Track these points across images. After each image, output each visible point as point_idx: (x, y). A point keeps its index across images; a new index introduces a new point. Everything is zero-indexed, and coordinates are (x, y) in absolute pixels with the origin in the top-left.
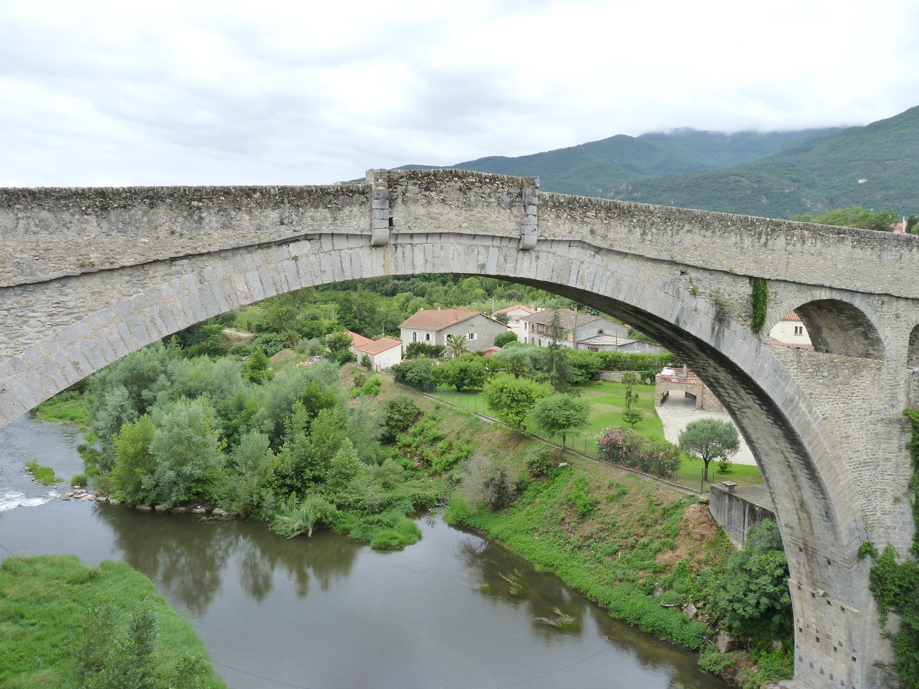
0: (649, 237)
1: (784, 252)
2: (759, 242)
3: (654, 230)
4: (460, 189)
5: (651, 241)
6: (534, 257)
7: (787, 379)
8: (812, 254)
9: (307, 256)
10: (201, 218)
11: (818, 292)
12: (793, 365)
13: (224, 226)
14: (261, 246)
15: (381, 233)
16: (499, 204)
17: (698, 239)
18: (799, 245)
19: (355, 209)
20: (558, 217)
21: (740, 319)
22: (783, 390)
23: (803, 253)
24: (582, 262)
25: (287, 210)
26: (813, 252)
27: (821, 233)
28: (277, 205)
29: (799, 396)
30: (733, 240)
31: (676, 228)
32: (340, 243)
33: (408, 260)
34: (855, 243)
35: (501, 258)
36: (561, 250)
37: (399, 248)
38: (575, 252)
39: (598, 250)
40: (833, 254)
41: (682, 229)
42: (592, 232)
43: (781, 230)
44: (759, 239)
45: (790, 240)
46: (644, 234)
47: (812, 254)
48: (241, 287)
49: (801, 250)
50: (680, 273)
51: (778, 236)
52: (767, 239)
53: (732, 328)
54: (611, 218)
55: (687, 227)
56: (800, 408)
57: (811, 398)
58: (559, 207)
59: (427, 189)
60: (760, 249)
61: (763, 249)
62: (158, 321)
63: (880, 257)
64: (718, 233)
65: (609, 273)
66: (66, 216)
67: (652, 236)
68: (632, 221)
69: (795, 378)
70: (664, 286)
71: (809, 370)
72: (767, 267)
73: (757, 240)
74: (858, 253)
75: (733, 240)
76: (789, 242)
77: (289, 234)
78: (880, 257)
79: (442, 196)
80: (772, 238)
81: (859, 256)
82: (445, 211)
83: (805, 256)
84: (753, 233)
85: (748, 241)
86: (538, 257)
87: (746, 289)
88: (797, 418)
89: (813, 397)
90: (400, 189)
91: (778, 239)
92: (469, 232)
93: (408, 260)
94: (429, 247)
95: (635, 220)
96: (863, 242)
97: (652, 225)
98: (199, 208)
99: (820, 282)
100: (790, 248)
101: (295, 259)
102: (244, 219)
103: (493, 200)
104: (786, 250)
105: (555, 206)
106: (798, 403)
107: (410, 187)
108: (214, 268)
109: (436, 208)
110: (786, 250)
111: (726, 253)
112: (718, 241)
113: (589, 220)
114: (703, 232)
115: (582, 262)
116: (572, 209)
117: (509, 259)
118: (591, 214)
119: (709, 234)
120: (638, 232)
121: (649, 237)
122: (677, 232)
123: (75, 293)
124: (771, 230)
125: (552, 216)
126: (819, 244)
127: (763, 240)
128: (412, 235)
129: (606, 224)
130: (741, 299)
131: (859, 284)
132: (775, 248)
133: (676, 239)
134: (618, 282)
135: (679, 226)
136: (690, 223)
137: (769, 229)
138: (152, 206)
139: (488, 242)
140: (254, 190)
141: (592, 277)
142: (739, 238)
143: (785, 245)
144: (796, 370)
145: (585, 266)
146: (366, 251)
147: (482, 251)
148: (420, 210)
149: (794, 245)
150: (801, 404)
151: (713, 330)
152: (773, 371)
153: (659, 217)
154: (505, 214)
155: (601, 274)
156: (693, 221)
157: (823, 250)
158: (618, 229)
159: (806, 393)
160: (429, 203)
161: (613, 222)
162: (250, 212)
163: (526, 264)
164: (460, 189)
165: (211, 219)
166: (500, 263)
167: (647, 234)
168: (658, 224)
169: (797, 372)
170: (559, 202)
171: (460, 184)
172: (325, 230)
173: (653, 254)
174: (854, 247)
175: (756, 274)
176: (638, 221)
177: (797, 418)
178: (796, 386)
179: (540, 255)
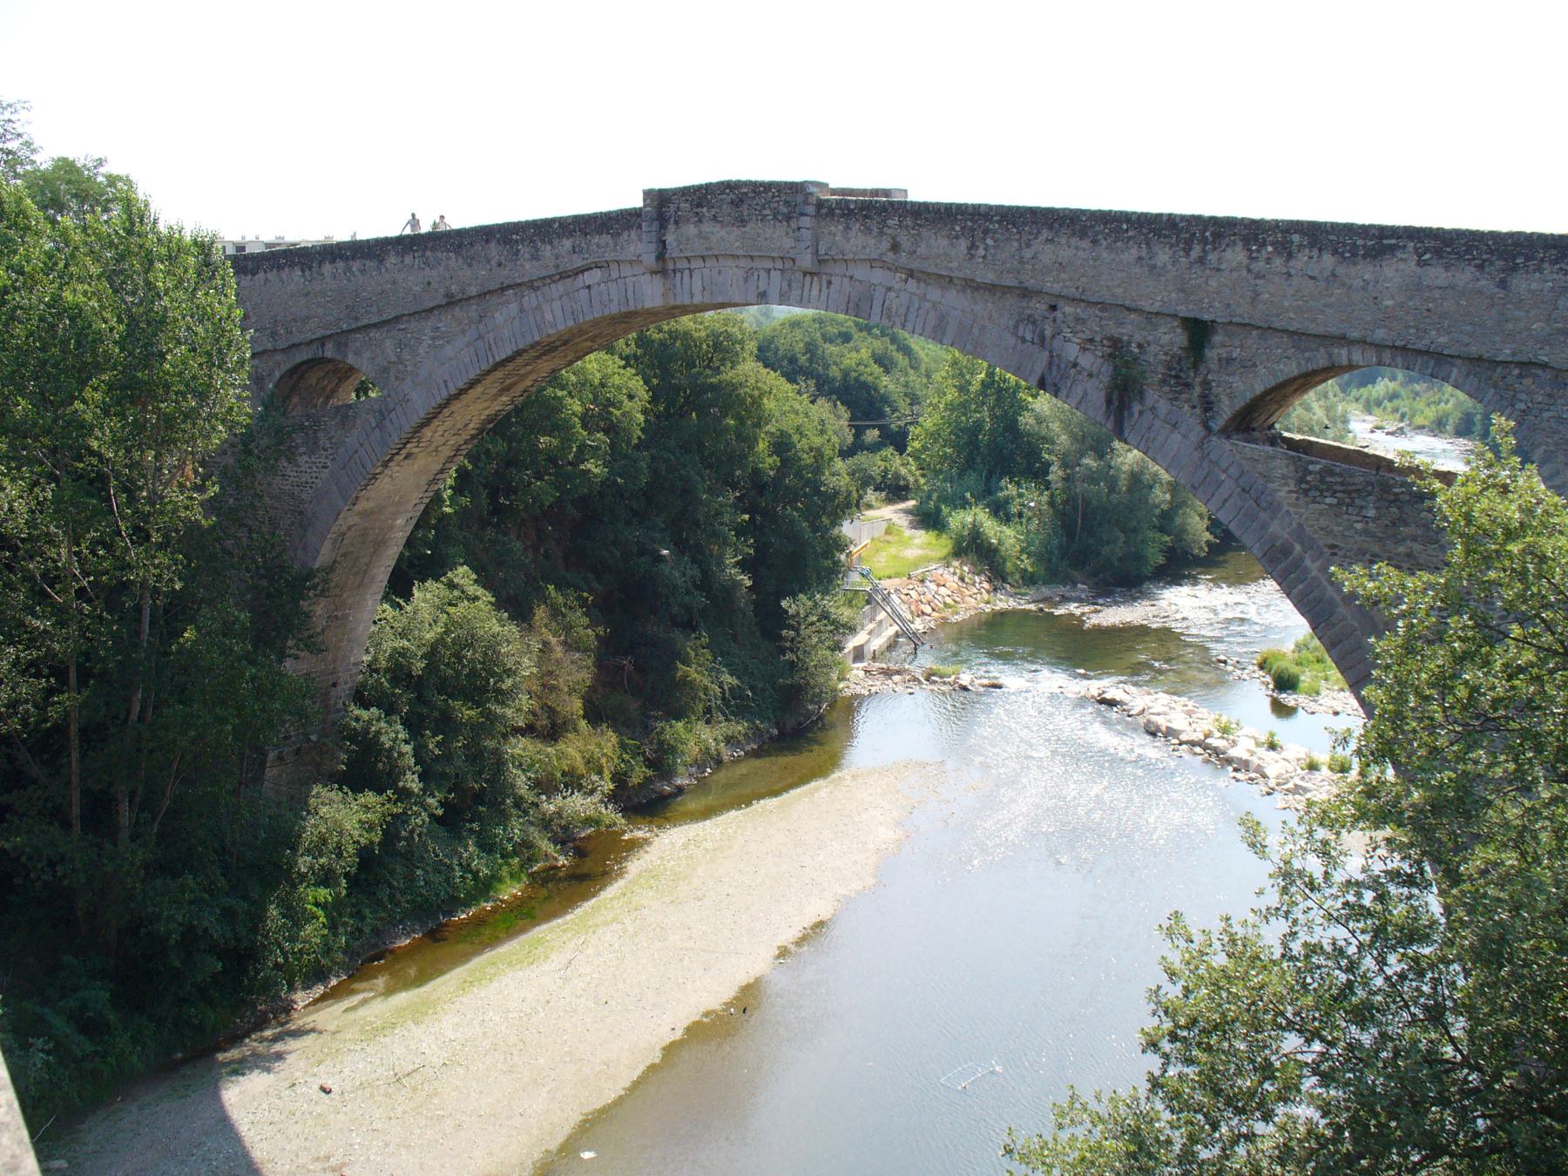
0: (981, 252)
1: (1245, 273)
2: (1188, 255)
3: (989, 242)
4: (732, 203)
5: (984, 257)
6: (824, 283)
7: (1274, 508)
8: (1311, 278)
9: (599, 284)
10: (518, 251)
11: (1344, 352)
12: (1286, 484)
13: (535, 257)
14: (564, 276)
15: (650, 259)
16: (775, 218)
17: (1065, 254)
18: (1278, 262)
19: (633, 233)
20: (847, 228)
21: (1166, 389)
22: (1264, 526)
23: (1289, 275)
24: (889, 289)
25: (578, 239)
26: (1315, 273)
27: (1331, 237)
28: (571, 235)
29: (1302, 544)
30: (1134, 252)
31: (1025, 238)
32: (626, 270)
33: (687, 287)
34: (1427, 256)
35: (785, 284)
36: (860, 272)
37: (678, 275)
38: (878, 276)
39: (911, 274)
40: (1367, 277)
41: (1036, 238)
42: (895, 247)
43: (1235, 234)
44: (1187, 252)
45: (1258, 251)
46: (973, 246)
47: (1311, 278)
48: (548, 317)
49: (1285, 270)
50: (1044, 307)
51: (1228, 245)
52: (1204, 250)
53: (1149, 402)
54: (920, 226)
55: (1046, 234)
56: (1306, 571)
57: (1335, 554)
58: (848, 215)
59: (699, 205)
60: (1190, 268)
61: (1197, 269)
62: (493, 347)
63: (1503, 284)
64: (1104, 243)
65: (928, 305)
66: (439, 254)
67: (986, 249)
68: (953, 229)
69: (1292, 510)
70: (1016, 327)
71: (1328, 500)
72: (1206, 301)
73: (1182, 253)
74: (1437, 275)
75: (1134, 252)
76: (1254, 255)
77: (578, 262)
78: (1503, 284)
79: (713, 211)
80: (1215, 249)
81: (1439, 282)
82: (717, 229)
83: (1295, 281)
84: (1174, 241)
85: (1163, 256)
86: (829, 283)
87: (1172, 338)
88: (1301, 587)
89: (1340, 553)
90: (672, 207)
91: (1229, 250)
92: (741, 252)
93: (687, 287)
94: (706, 271)
95: (957, 228)
96: (1450, 253)
97: (986, 232)
98: (516, 241)
99: (1333, 330)
100: (1260, 266)
101: (589, 287)
102: (546, 251)
103: (767, 212)
104: (1249, 271)
105: (843, 215)
106: (1302, 559)
107: (682, 205)
108: (530, 299)
109: (707, 227)
110: (1249, 271)
111: (1119, 275)
112: (1105, 254)
113: (890, 231)
114: (1074, 241)
115: (889, 289)
116: (866, 217)
117: (793, 284)
118: (890, 222)
119: (1086, 244)
120: (963, 244)
121: (981, 252)
122: (1028, 246)
123: (445, 322)
124: (1213, 234)
125: (841, 227)
126: (1328, 260)
127: (1196, 251)
128: (688, 259)
129: (913, 235)
130: (1166, 354)
131: (1441, 340)
132: (1222, 267)
133: (1027, 254)
134: (942, 318)
135: (1030, 234)
136: (1051, 228)
137: (1207, 234)
138: (487, 241)
139: (769, 265)
140: (553, 220)
141: (903, 311)
142: (1144, 253)
143: (1246, 261)
144: (1295, 495)
145: (892, 295)
146: (647, 277)
147: (763, 274)
148: (691, 229)
149: (1268, 261)
150: (1308, 562)
151: (1109, 402)
152: (1239, 490)
153: (997, 222)
154: (781, 229)
155: (917, 306)
156: (1056, 225)
157: (1340, 271)
158: (932, 242)
159: (1321, 543)
160: (700, 221)
161: (923, 231)
162: (550, 243)
163: (815, 292)
164: (732, 203)
165: (525, 250)
166: (784, 290)
167: (978, 247)
168: (995, 232)
169: (1297, 499)
170: (849, 209)
171: (732, 196)
172: (609, 256)
173: (990, 277)
174: (1420, 264)
175: (1183, 311)
176: (963, 228)
177: (1301, 587)
178: (1294, 525)
179: (833, 279)
